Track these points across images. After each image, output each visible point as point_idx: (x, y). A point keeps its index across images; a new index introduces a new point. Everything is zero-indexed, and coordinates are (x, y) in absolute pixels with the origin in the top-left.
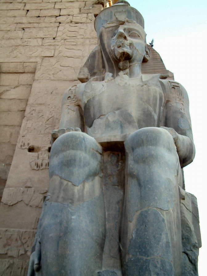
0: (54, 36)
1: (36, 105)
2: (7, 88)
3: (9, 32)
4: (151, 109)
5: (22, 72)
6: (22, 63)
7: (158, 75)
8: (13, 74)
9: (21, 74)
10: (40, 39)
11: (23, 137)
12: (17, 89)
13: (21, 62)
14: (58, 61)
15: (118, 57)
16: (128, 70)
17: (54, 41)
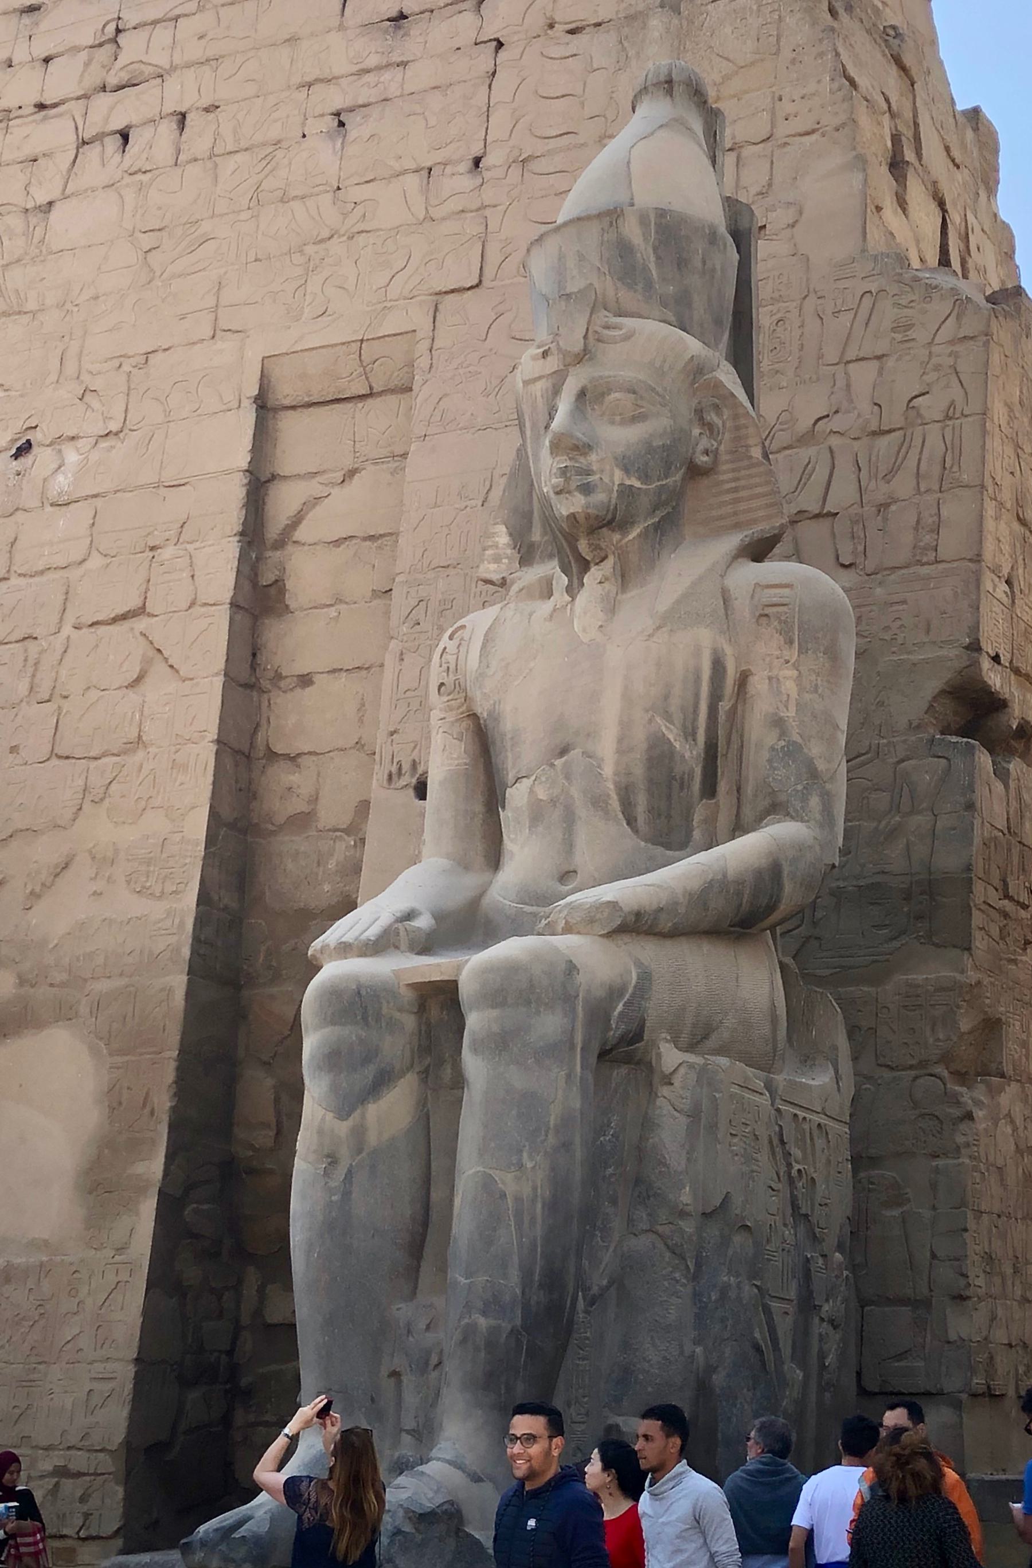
0: (476, 150)
1: (431, 575)
3: (280, 154)
4: (672, 734)
9: (360, 405)
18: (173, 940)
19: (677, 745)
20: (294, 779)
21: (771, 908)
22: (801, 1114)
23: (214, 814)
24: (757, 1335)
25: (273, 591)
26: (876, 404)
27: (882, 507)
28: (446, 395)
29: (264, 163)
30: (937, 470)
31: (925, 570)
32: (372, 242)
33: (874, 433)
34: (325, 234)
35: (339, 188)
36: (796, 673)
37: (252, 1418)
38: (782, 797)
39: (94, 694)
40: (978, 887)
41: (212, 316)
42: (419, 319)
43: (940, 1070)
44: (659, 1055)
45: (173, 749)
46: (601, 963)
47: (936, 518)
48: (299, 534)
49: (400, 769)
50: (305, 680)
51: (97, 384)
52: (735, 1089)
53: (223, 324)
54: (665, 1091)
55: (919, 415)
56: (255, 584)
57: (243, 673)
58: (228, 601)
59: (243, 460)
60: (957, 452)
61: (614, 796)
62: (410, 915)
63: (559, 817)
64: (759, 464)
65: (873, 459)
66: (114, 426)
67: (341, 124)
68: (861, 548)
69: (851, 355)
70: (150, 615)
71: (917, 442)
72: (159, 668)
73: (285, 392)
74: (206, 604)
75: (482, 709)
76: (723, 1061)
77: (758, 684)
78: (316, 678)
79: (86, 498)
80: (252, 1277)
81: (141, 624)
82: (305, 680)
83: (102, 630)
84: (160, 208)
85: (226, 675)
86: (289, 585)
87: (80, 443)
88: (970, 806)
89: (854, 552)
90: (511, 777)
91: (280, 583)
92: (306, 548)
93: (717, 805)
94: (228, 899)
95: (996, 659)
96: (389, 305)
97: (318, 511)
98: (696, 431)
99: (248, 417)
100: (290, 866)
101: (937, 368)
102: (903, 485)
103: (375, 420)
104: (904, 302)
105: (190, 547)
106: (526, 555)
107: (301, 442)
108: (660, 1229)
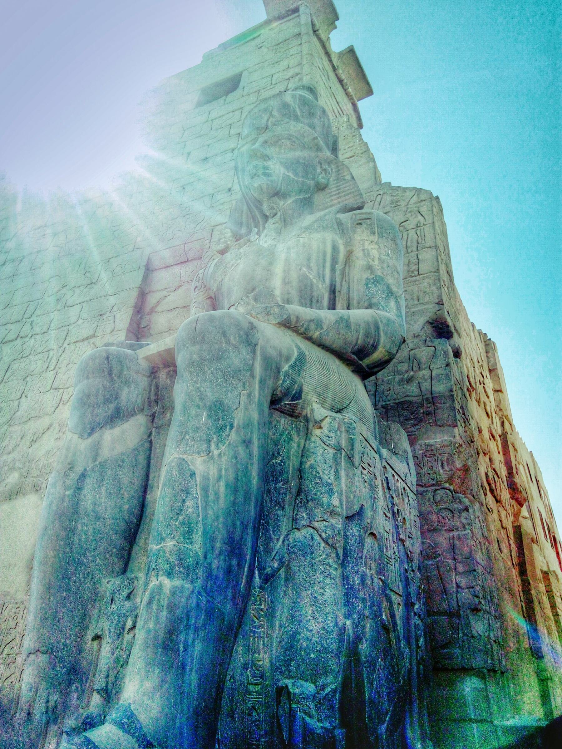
0: (230, 186)
5: (185, 260)
19: (315, 281)
24: (384, 617)
25: (146, 329)
30: (415, 245)
36: (377, 247)
38: (375, 300)
47: (417, 260)
54: (317, 432)
64: (349, 181)
67: (184, 188)
73: (156, 263)
86: (152, 326)
91: (149, 327)
97: (166, 300)
99: (142, 271)
108: (316, 525)
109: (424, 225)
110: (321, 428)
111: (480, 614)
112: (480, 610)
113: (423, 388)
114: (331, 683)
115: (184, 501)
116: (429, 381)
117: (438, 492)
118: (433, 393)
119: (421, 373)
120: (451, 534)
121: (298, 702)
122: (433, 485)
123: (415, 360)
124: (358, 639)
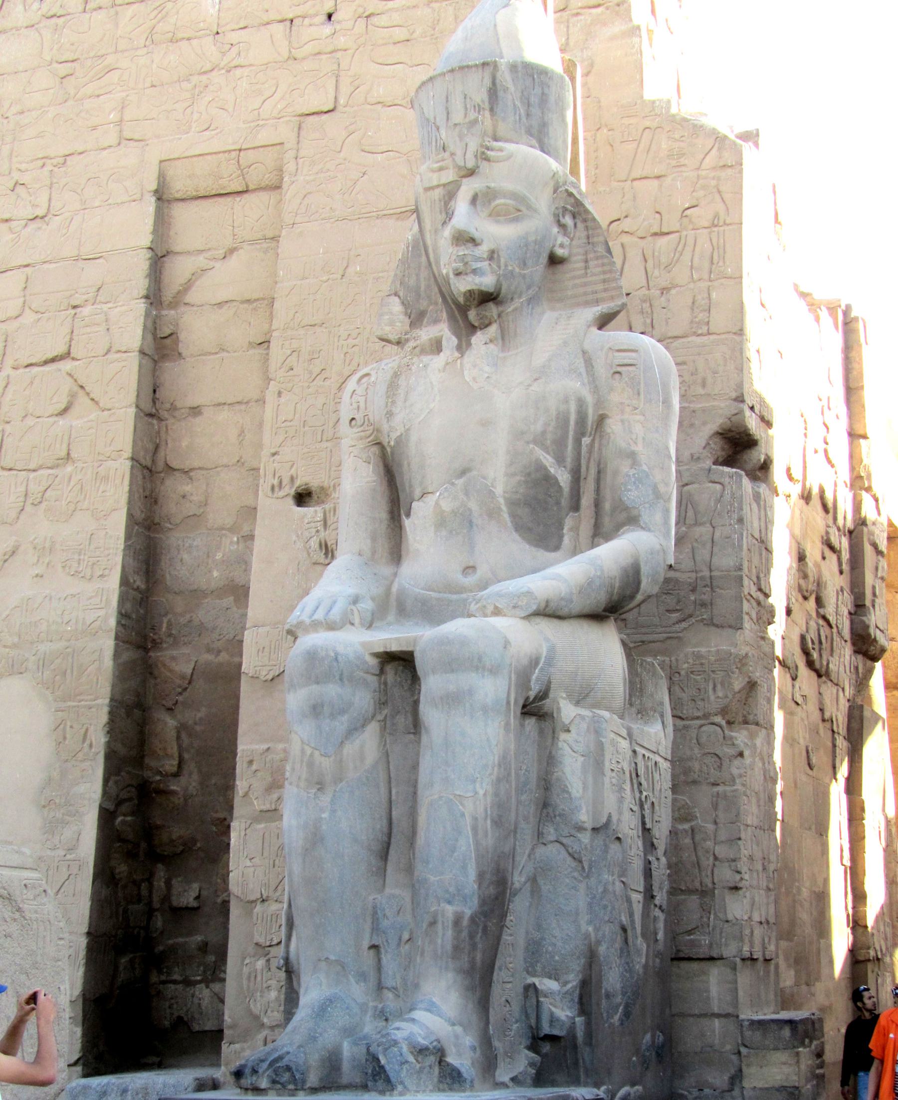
0: (328, 7)
1: (302, 332)
2: (201, 261)
4: (548, 461)
5: (240, 189)
6: (234, 154)
7: (591, 313)
8: (211, 200)
9: (238, 199)
10: (281, 26)
11: (274, 454)
12: (233, 261)
13: (230, 151)
14: (352, 128)
15: (461, 300)
16: (493, 329)
17: (328, 29)
18: (102, 613)
19: (552, 470)
20: (188, 488)
21: (632, 597)
22: (647, 754)
23: (130, 516)
24: (623, 919)
25: (168, 342)
26: (657, 212)
27: (664, 290)
28: (310, 193)
29: (156, 12)
30: (706, 264)
31: (699, 340)
32: (246, 74)
33: (655, 234)
34: (208, 67)
35: (218, 33)
37: (163, 978)
39: (30, 421)
40: (746, 582)
41: (118, 128)
42: (285, 133)
43: (718, 719)
44: (559, 709)
45: (96, 464)
46: (523, 637)
47: (707, 301)
48: (188, 298)
49: (281, 483)
50: (196, 411)
51: (26, 178)
52: (612, 735)
53: (127, 134)
54: (563, 736)
55: (691, 222)
56: (154, 335)
57: (147, 406)
58: (138, 349)
59: (146, 240)
60: (721, 251)
61: (504, 508)
62: (355, 600)
63: (459, 525)
64: (602, 257)
65: (656, 254)
66: (40, 212)
68: (649, 321)
69: (635, 175)
70: (73, 359)
71: (690, 242)
72: (82, 399)
73: (179, 186)
74: (119, 351)
75: (390, 441)
76: (606, 714)
77: (613, 426)
78: (205, 411)
79: (19, 267)
80: (161, 872)
81: (66, 366)
82: (196, 411)
83: (36, 370)
84: (72, 44)
85: (137, 406)
86: (182, 336)
87: (13, 224)
88: (740, 521)
89: (645, 323)
90: (417, 493)
91: (174, 336)
92: (195, 308)
93: (579, 517)
94: (140, 583)
95: (752, 408)
96: (261, 123)
98: (555, 230)
99: (150, 205)
100: (185, 556)
101: (704, 187)
102: (681, 274)
103: (251, 212)
104: (677, 136)
105: (105, 307)
106: (417, 319)
107: (193, 226)
108: (564, 841)
109: (725, 224)
110: (569, 731)
111: (741, 892)
112: (741, 888)
113: (698, 558)
114: (573, 980)
115: (457, 840)
116: (709, 545)
117: (704, 728)
118: (713, 568)
119: (698, 530)
120: (716, 789)
121: (546, 996)
122: (698, 718)
123: (690, 506)
124: (598, 942)
